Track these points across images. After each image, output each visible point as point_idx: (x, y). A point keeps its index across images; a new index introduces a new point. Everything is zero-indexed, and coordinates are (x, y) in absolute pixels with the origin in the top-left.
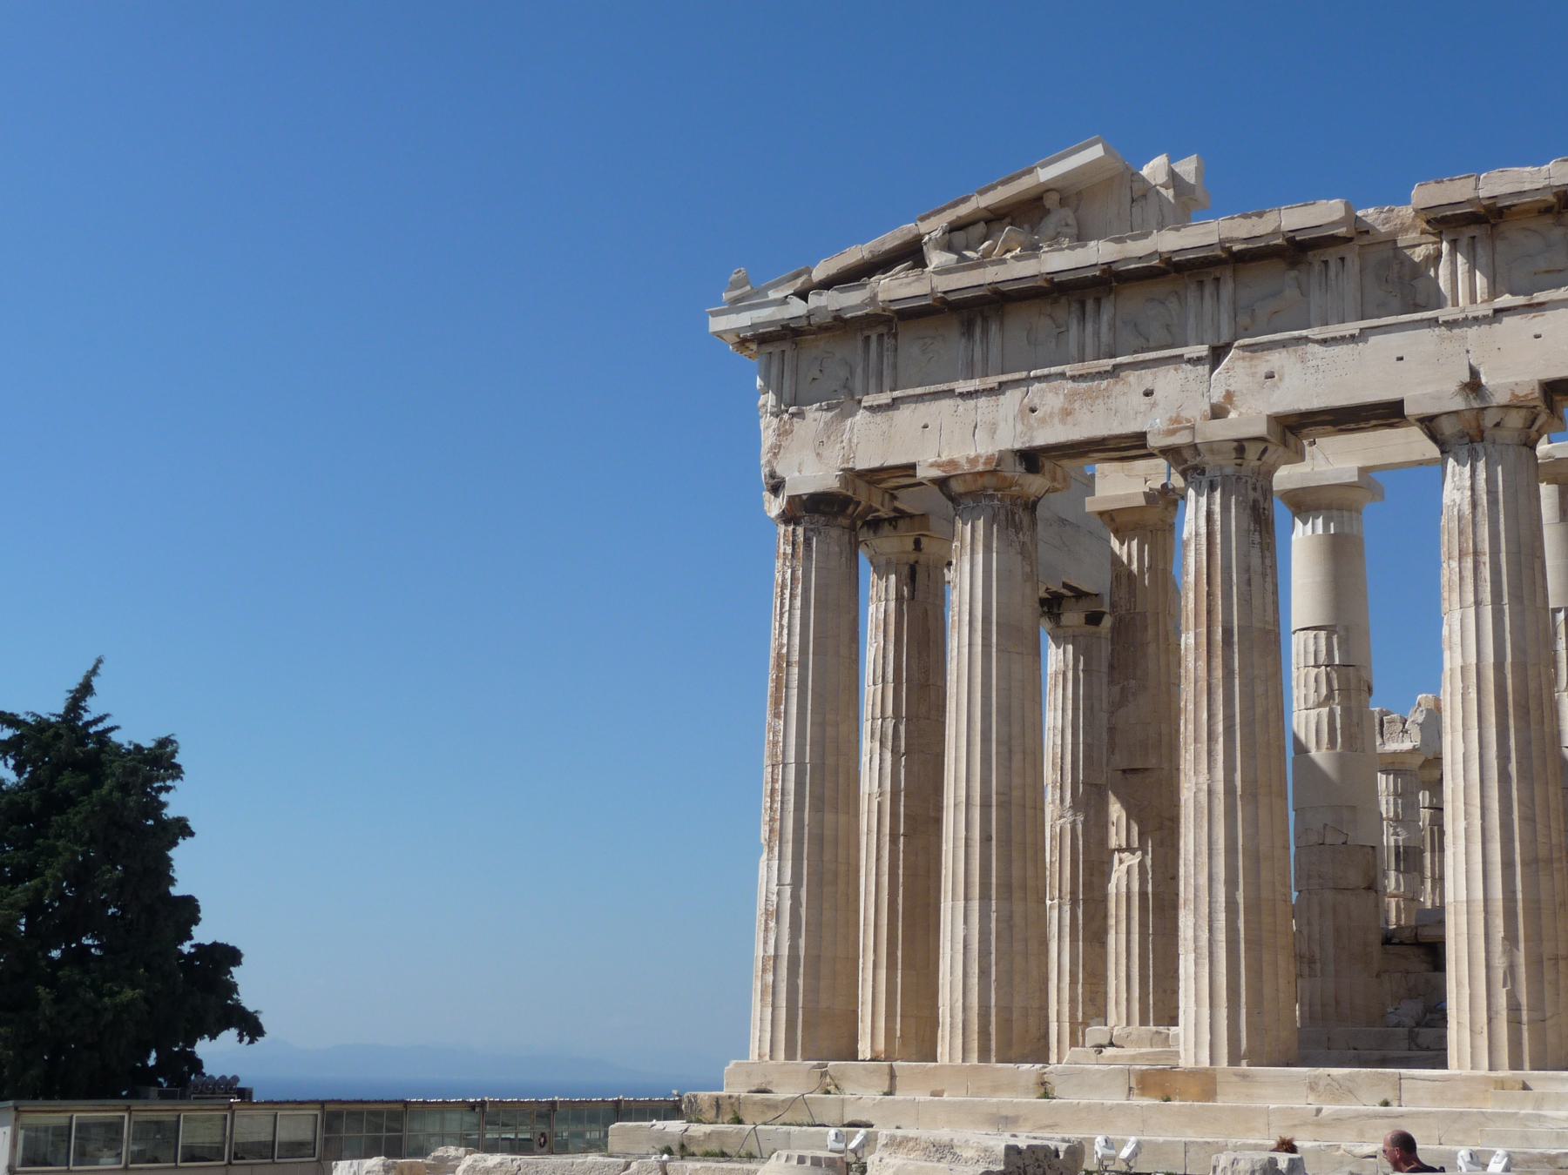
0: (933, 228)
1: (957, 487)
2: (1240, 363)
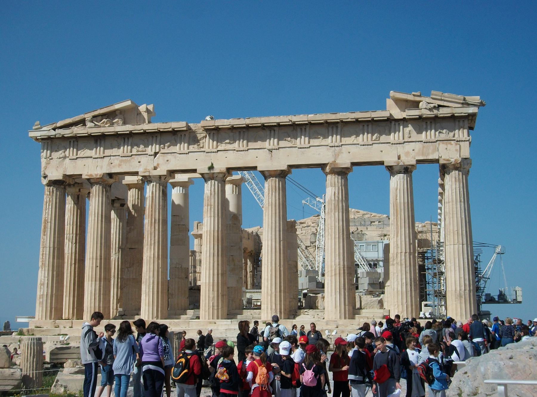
0: (88, 116)
1: (92, 181)
2: (161, 157)
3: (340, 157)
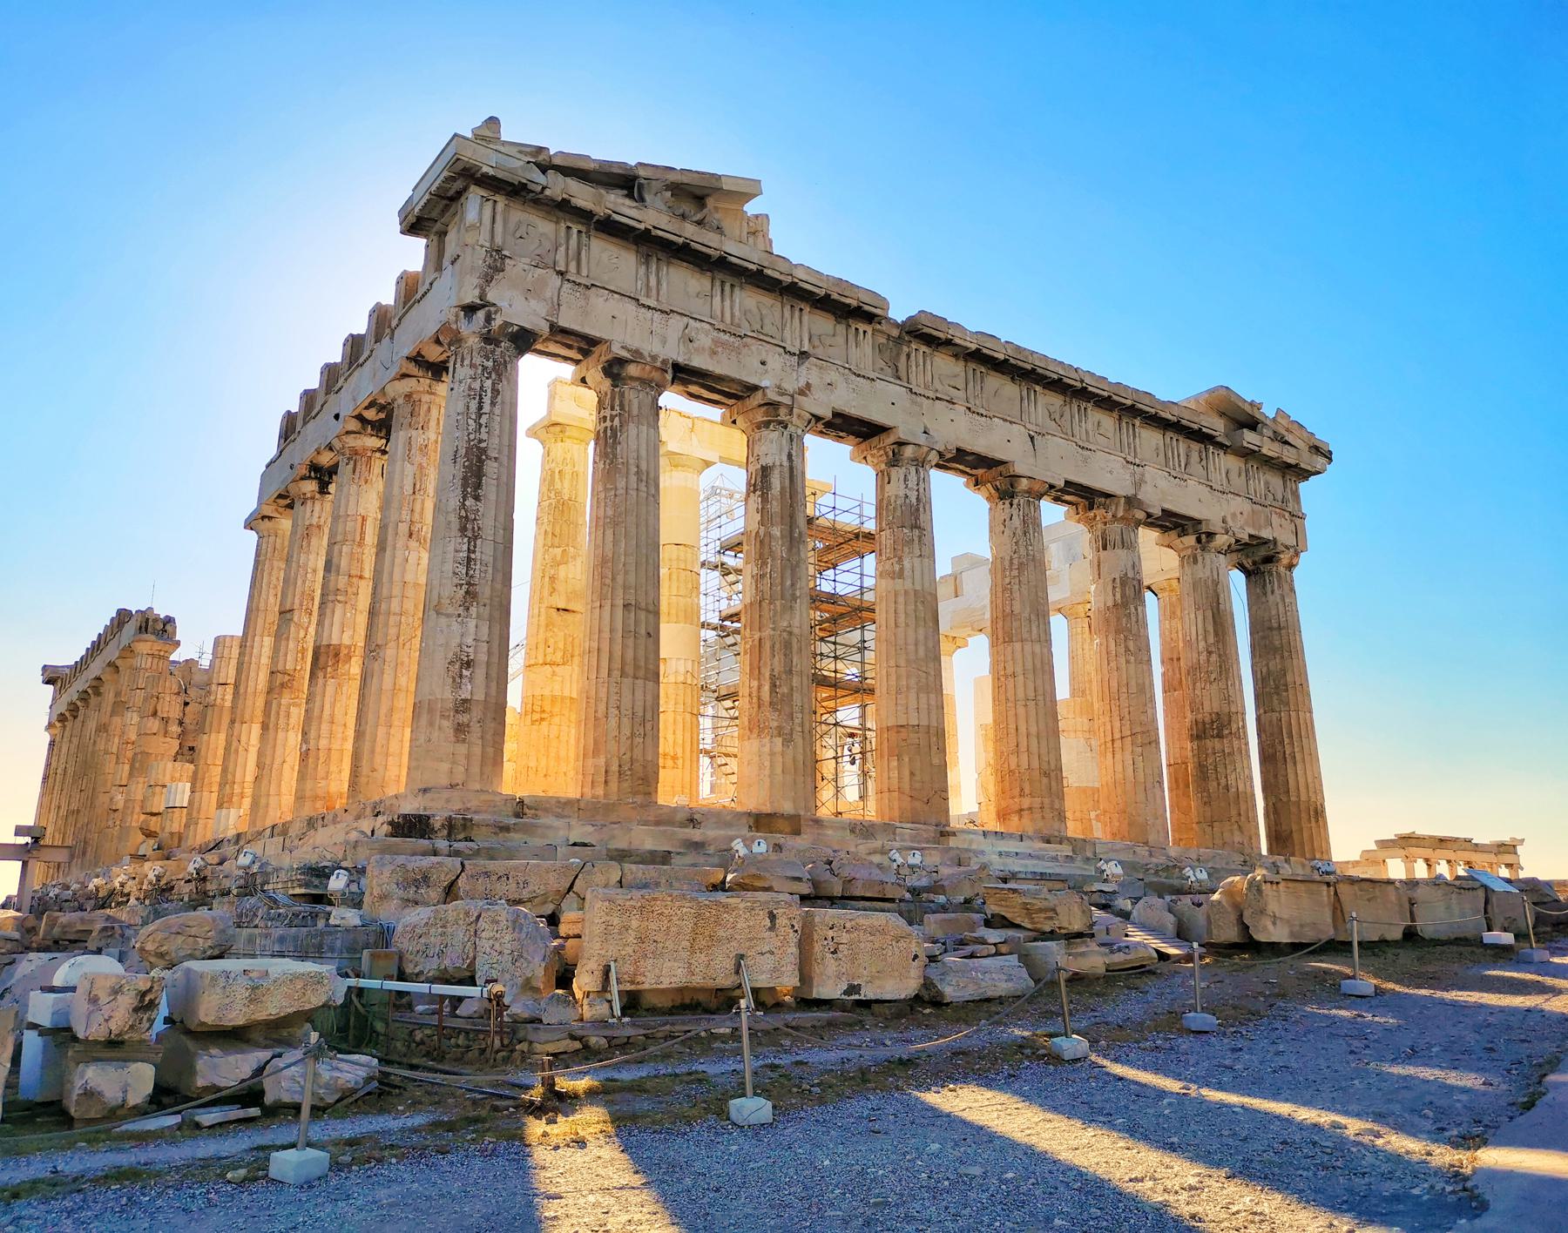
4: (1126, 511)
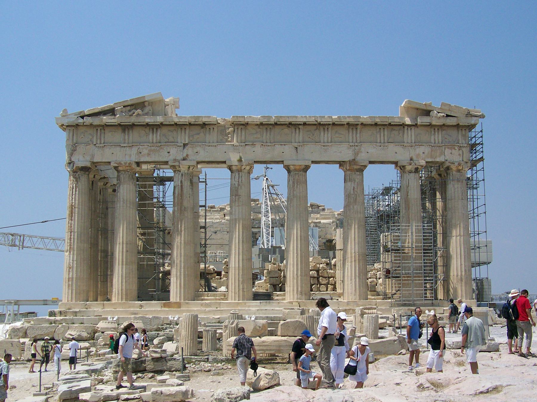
1: (120, 168)
3: (359, 155)
4: (350, 166)
